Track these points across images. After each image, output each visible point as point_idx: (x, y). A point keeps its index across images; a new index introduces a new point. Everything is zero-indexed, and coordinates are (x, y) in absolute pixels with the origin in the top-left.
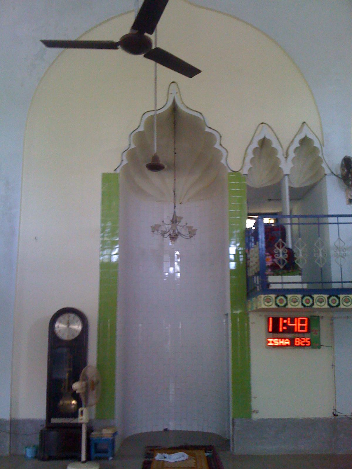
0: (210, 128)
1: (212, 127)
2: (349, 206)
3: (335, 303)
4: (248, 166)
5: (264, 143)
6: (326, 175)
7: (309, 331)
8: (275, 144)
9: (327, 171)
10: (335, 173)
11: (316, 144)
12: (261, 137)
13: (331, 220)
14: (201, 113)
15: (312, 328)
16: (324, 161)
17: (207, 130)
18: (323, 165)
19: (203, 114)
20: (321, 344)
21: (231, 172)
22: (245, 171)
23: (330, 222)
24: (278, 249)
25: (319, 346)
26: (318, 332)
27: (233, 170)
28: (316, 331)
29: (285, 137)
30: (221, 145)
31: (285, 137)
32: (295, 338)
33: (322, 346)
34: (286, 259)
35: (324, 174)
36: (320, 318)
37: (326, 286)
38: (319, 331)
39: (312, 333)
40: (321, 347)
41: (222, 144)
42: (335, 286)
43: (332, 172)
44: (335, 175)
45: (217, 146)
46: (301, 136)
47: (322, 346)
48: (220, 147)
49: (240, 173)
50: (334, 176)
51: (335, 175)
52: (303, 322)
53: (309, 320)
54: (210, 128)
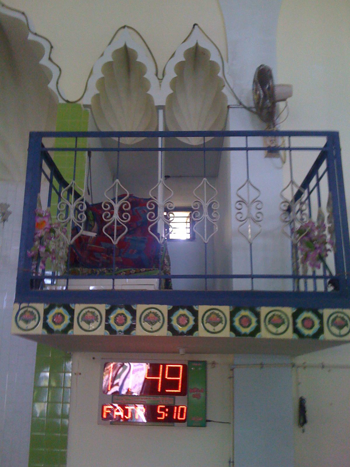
0: (36, 34)
1: (38, 33)
2: (268, 159)
3: (63, 317)
4: (93, 91)
5: (126, 58)
6: (229, 107)
7: (184, 393)
8: (142, 57)
9: (231, 101)
10: (245, 104)
11: (214, 57)
12: (121, 45)
13: (234, 142)
14: (23, 13)
15: (191, 385)
16: (226, 84)
17: (31, 37)
18: (225, 91)
19: (26, 13)
20: (208, 418)
21: (64, 102)
22: (87, 100)
23: (232, 146)
24: (123, 223)
25: (204, 422)
26: (202, 394)
27: (67, 98)
28: (198, 390)
29: (162, 51)
30: (50, 59)
31: (162, 51)
32: (158, 406)
33: (210, 421)
34: (126, 224)
35: (226, 107)
36: (209, 367)
37: (219, 285)
38: (205, 390)
39: (190, 395)
40: (208, 423)
41: (52, 57)
42: (240, 285)
43: (241, 103)
44: (245, 107)
45: (44, 61)
46: (190, 44)
47: (210, 421)
48: (49, 62)
49: (80, 105)
50: (244, 110)
51: (245, 107)
52: (174, 372)
53: (185, 367)
54: (36, 34)
